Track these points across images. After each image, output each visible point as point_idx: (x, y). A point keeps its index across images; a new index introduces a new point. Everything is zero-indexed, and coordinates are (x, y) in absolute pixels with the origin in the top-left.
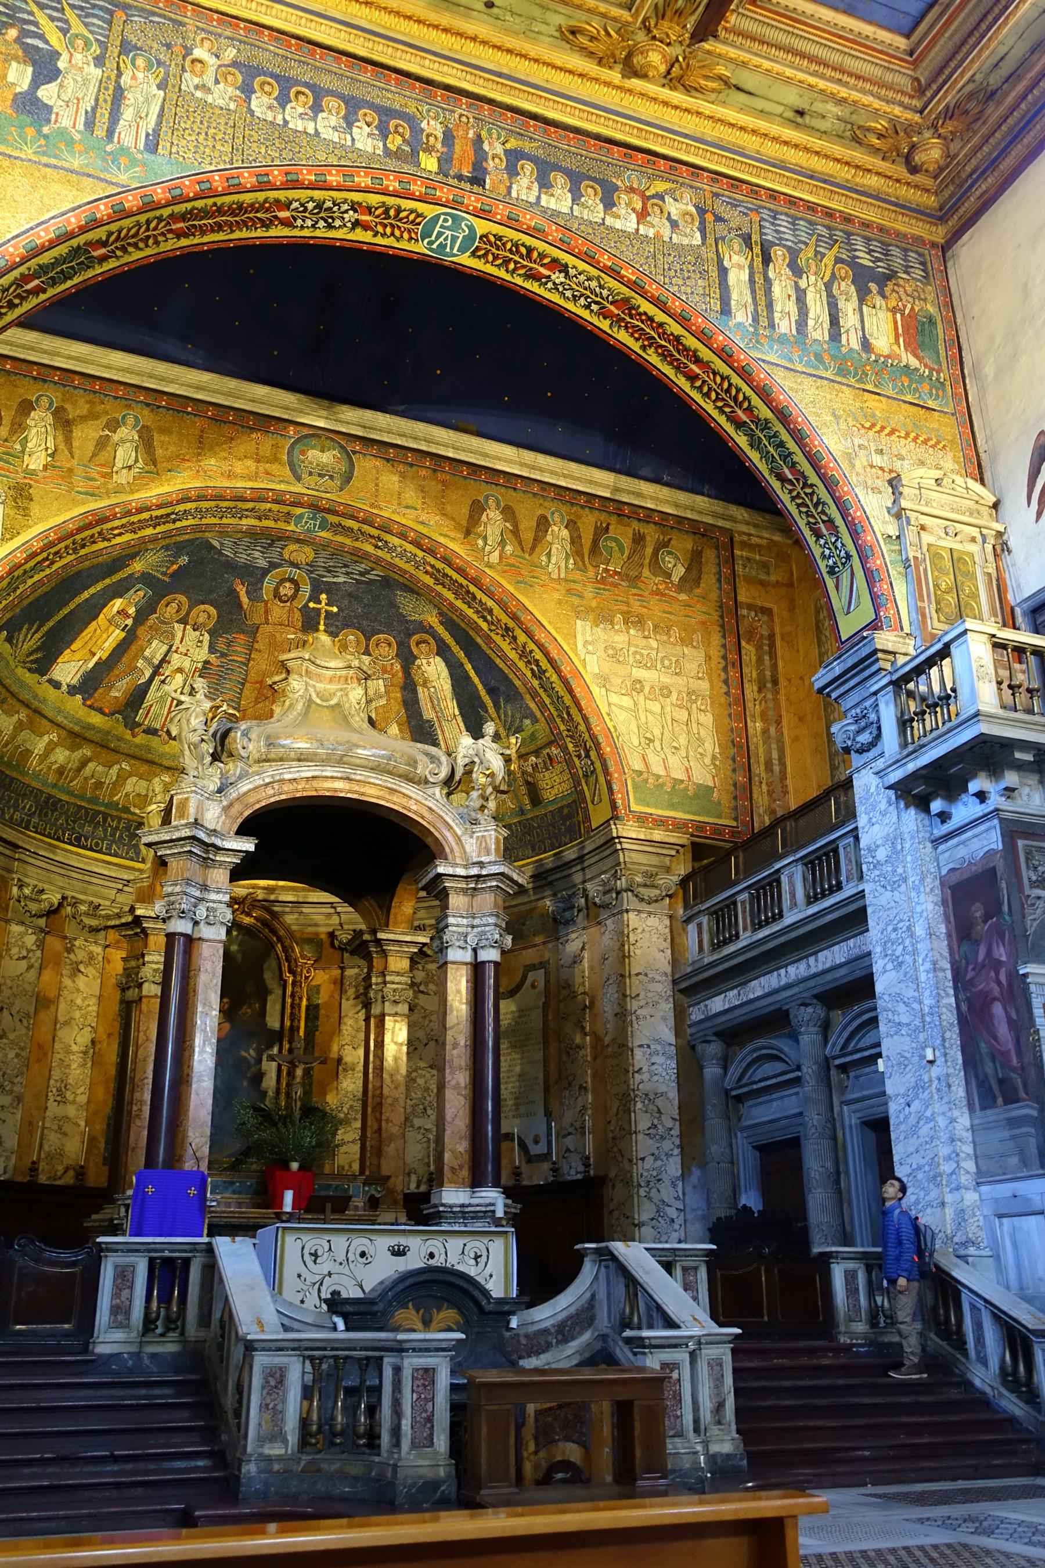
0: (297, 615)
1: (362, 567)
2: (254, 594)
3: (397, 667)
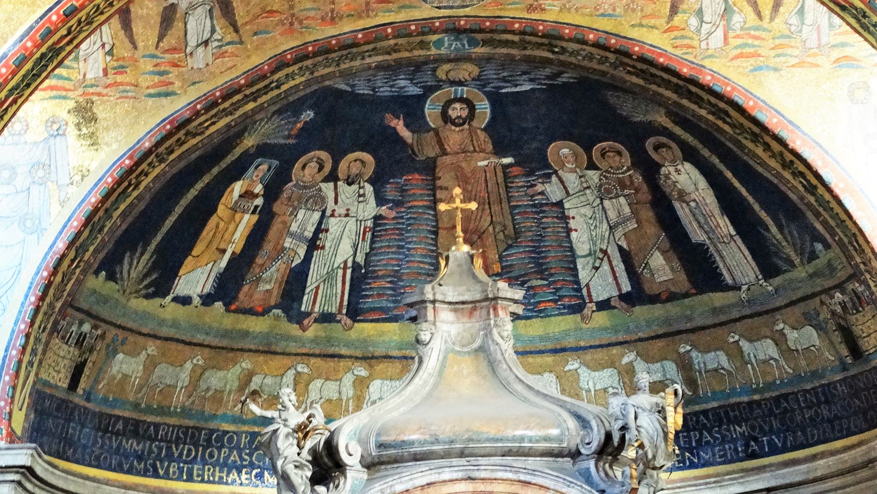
0: (482, 136)
1: (548, 71)
2: (416, 121)
3: (638, 179)
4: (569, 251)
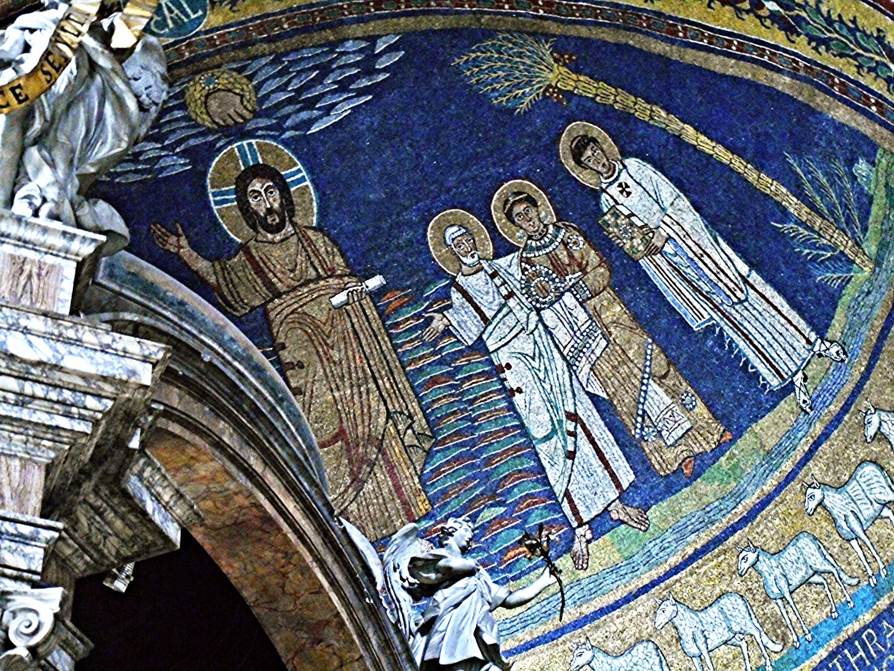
0: (320, 241)
4: (521, 436)
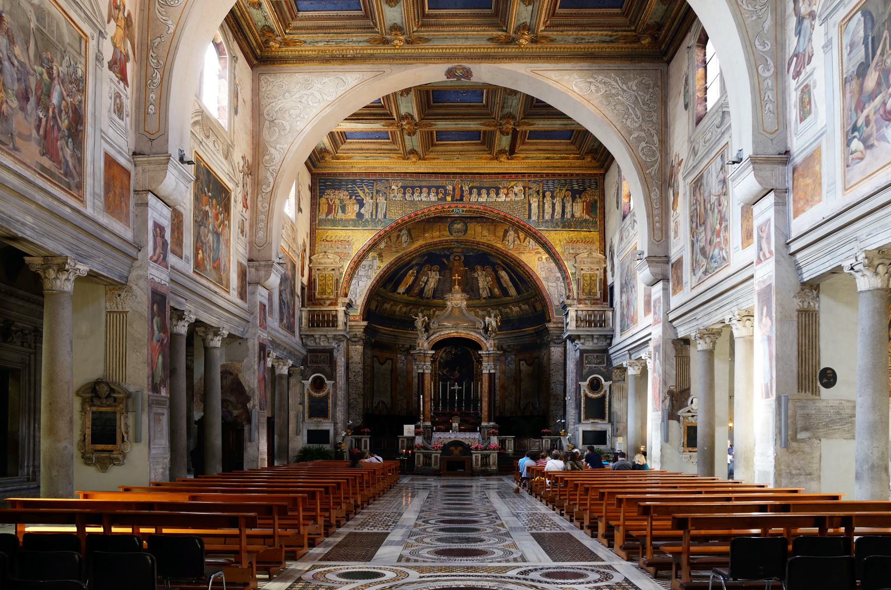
2: (448, 259)
